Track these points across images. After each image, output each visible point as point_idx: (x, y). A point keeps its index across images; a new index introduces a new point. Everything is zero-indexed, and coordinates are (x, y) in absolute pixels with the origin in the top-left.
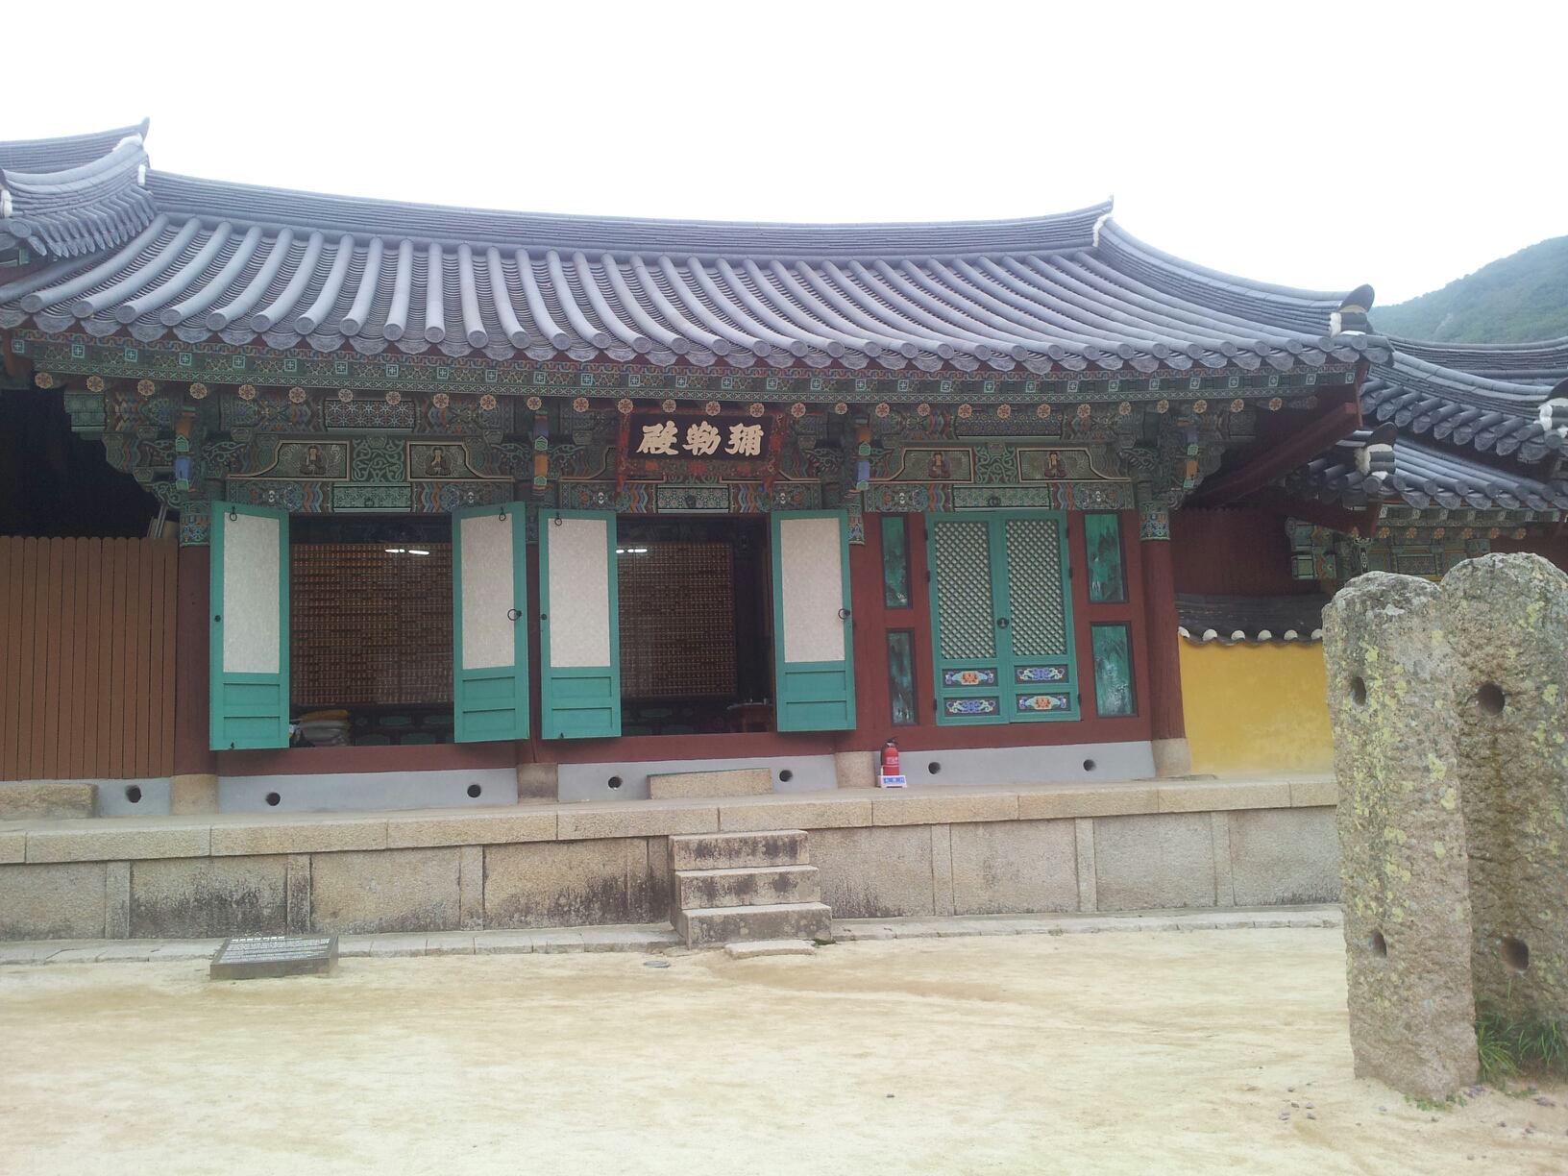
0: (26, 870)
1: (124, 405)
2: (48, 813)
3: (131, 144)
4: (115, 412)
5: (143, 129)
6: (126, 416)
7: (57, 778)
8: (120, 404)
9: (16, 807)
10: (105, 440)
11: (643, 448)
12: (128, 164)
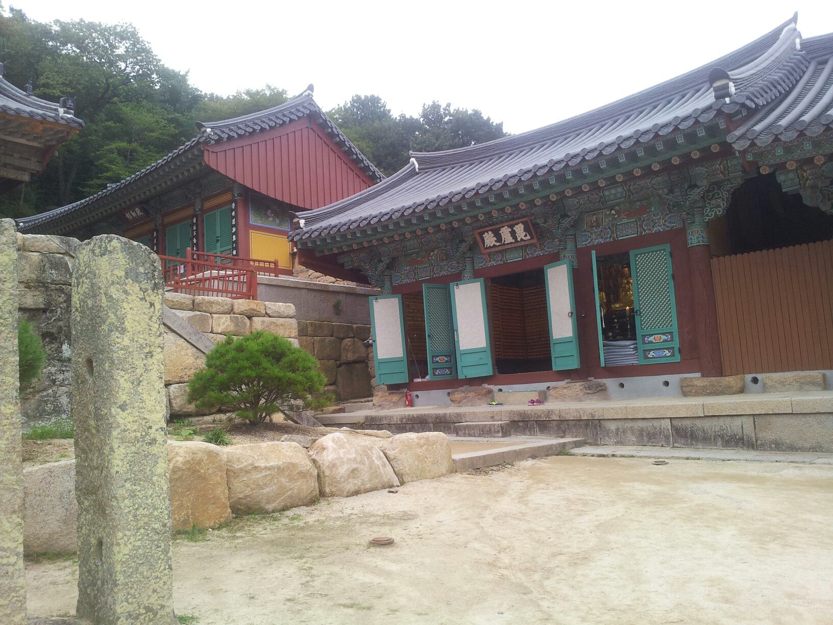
0: (794, 417)
1: (808, 171)
2: (800, 389)
3: (790, 30)
4: (804, 177)
5: (794, 19)
6: (810, 177)
7: (803, 370)
8: (806, 172)
9: (784, 385)
10: (801, 192)
12: (789, 42)
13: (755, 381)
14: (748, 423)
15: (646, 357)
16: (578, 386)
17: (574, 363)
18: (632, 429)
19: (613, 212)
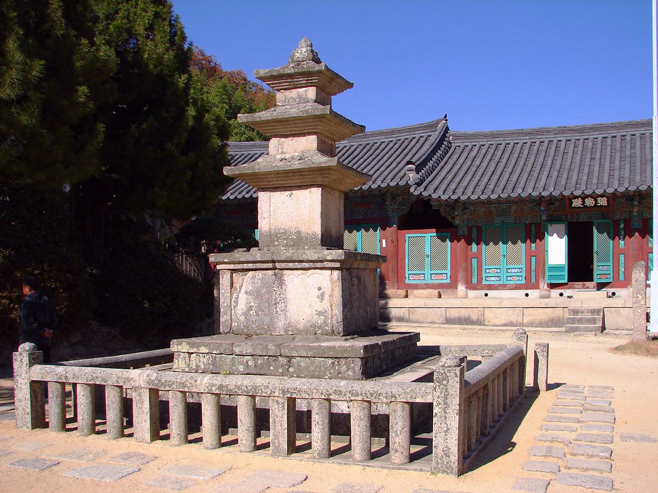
11: (573, 205)
19: (352, 203)
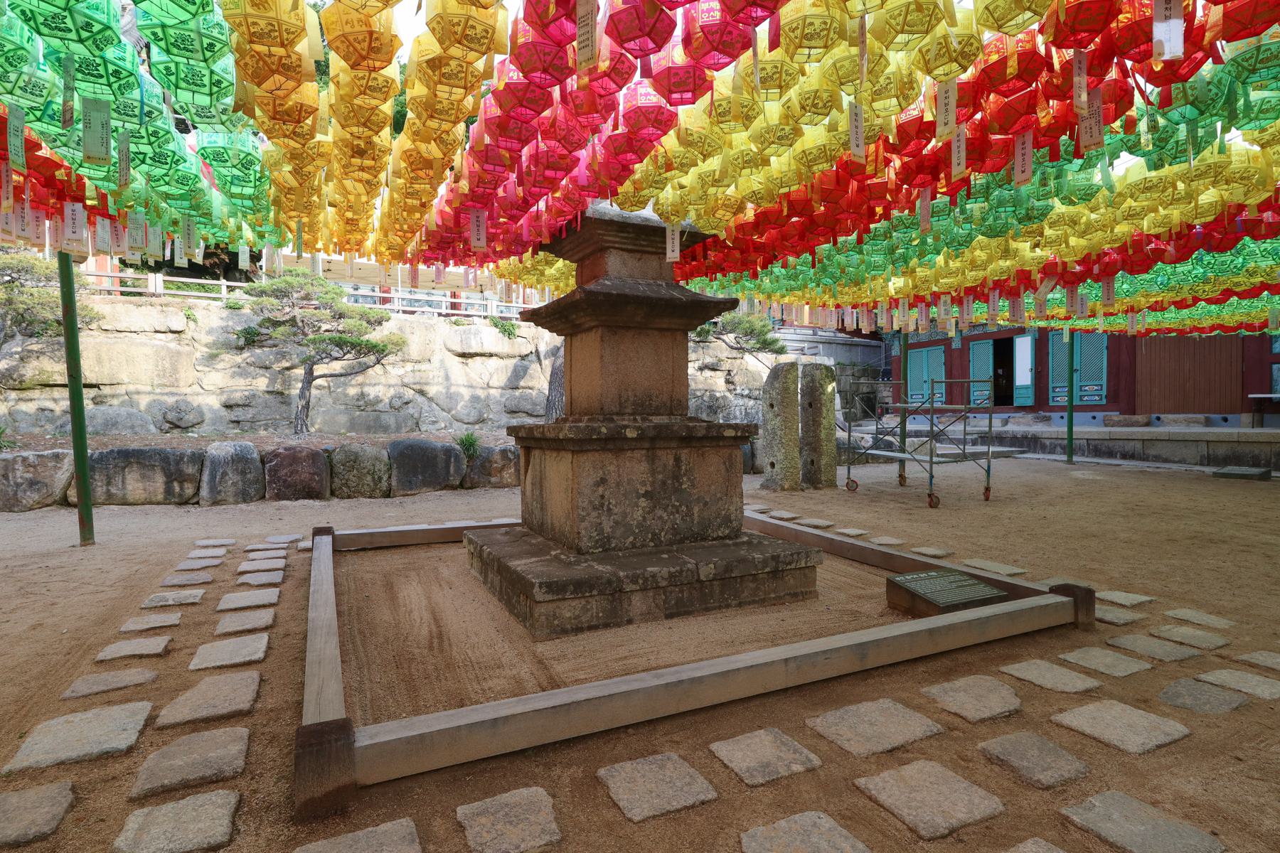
13: (1158, 419)
14: (1139, 445)
15: (1081, 400)
16: (1030, 416)
17: (1030, 402)
18: (1060, 445)
